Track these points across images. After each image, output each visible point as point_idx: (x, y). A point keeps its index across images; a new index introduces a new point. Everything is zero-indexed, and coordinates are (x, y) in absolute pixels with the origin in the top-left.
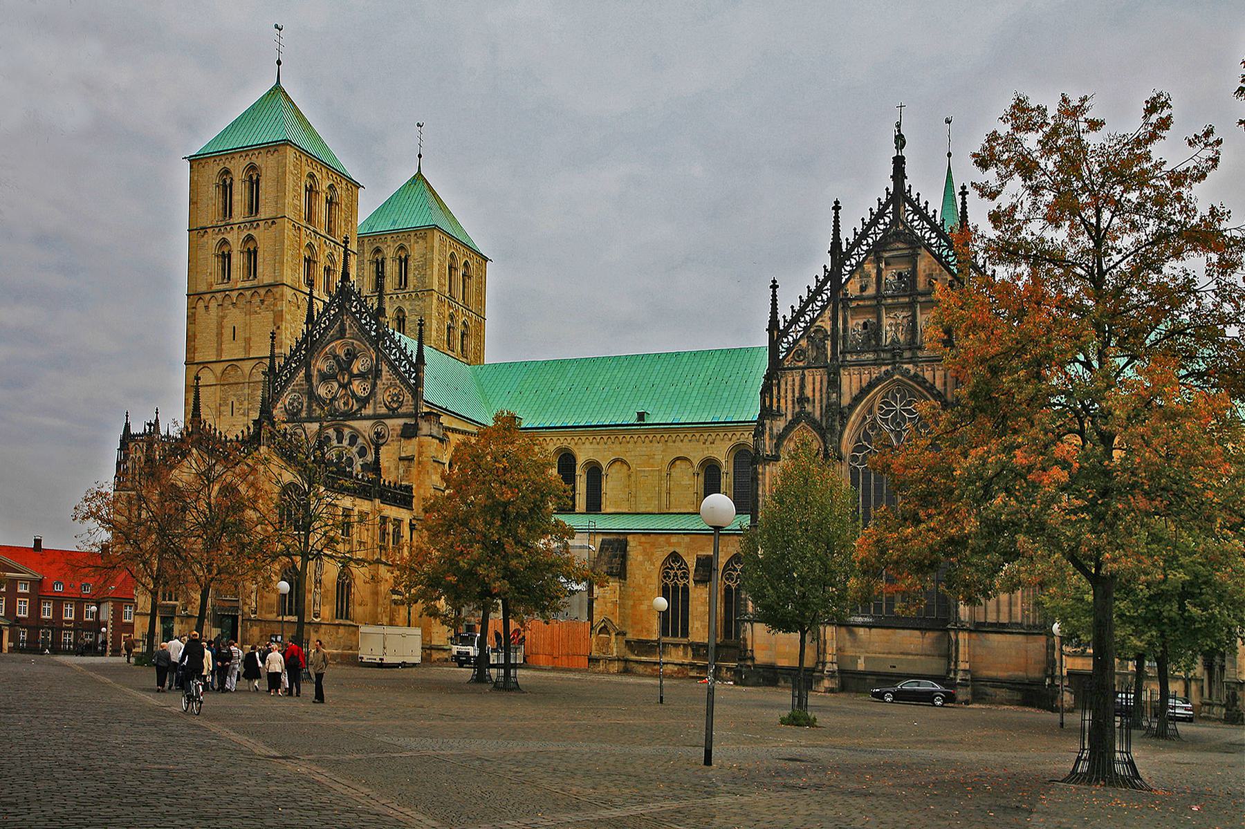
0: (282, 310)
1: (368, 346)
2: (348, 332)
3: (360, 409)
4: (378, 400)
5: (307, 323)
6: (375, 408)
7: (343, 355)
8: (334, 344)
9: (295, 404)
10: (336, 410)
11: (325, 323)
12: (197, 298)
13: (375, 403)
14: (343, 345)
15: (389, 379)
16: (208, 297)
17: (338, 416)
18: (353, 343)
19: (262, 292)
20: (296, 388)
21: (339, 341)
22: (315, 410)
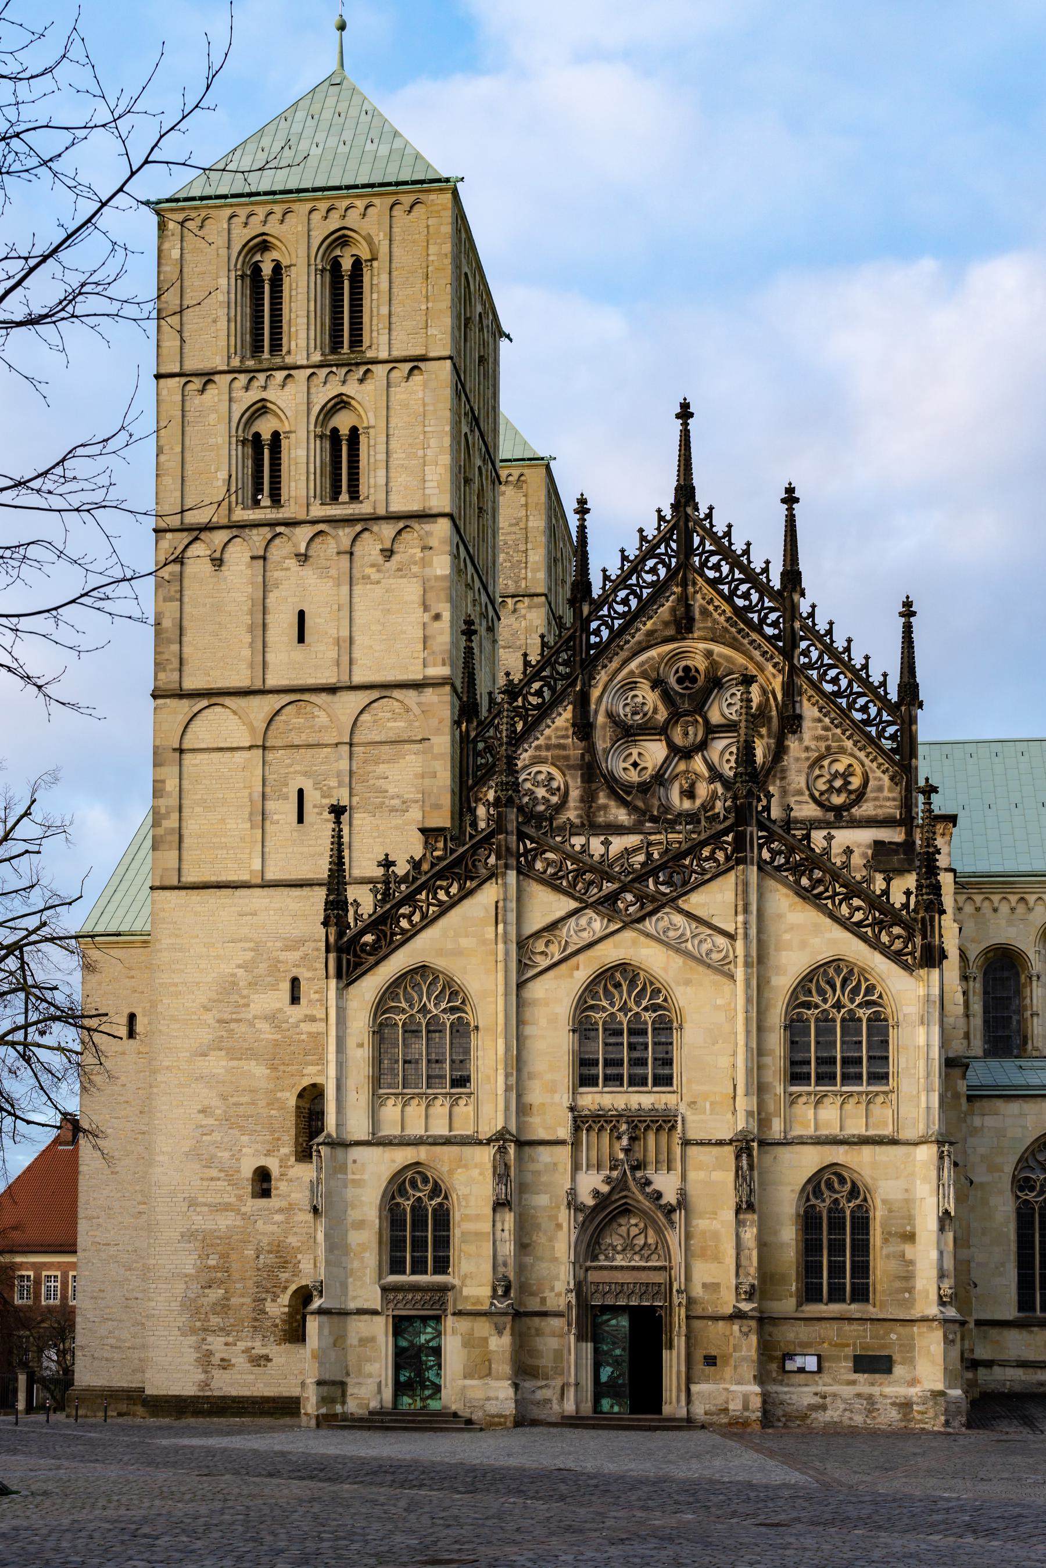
1: (760, 659)
2: (698, 624)
4: (793, 787)
5: (573, 602)
7: (672, 680)
8: (653, 653)
9: (541, 792)
10: (666, 808)
12: (185, 538)
13: (784, 792)
14: (675, 657)
15: (818, 738)
16: (221, 536)
18: (709, 654)
19: (388, 530)
20: (544, 753)
22: (605, 807)
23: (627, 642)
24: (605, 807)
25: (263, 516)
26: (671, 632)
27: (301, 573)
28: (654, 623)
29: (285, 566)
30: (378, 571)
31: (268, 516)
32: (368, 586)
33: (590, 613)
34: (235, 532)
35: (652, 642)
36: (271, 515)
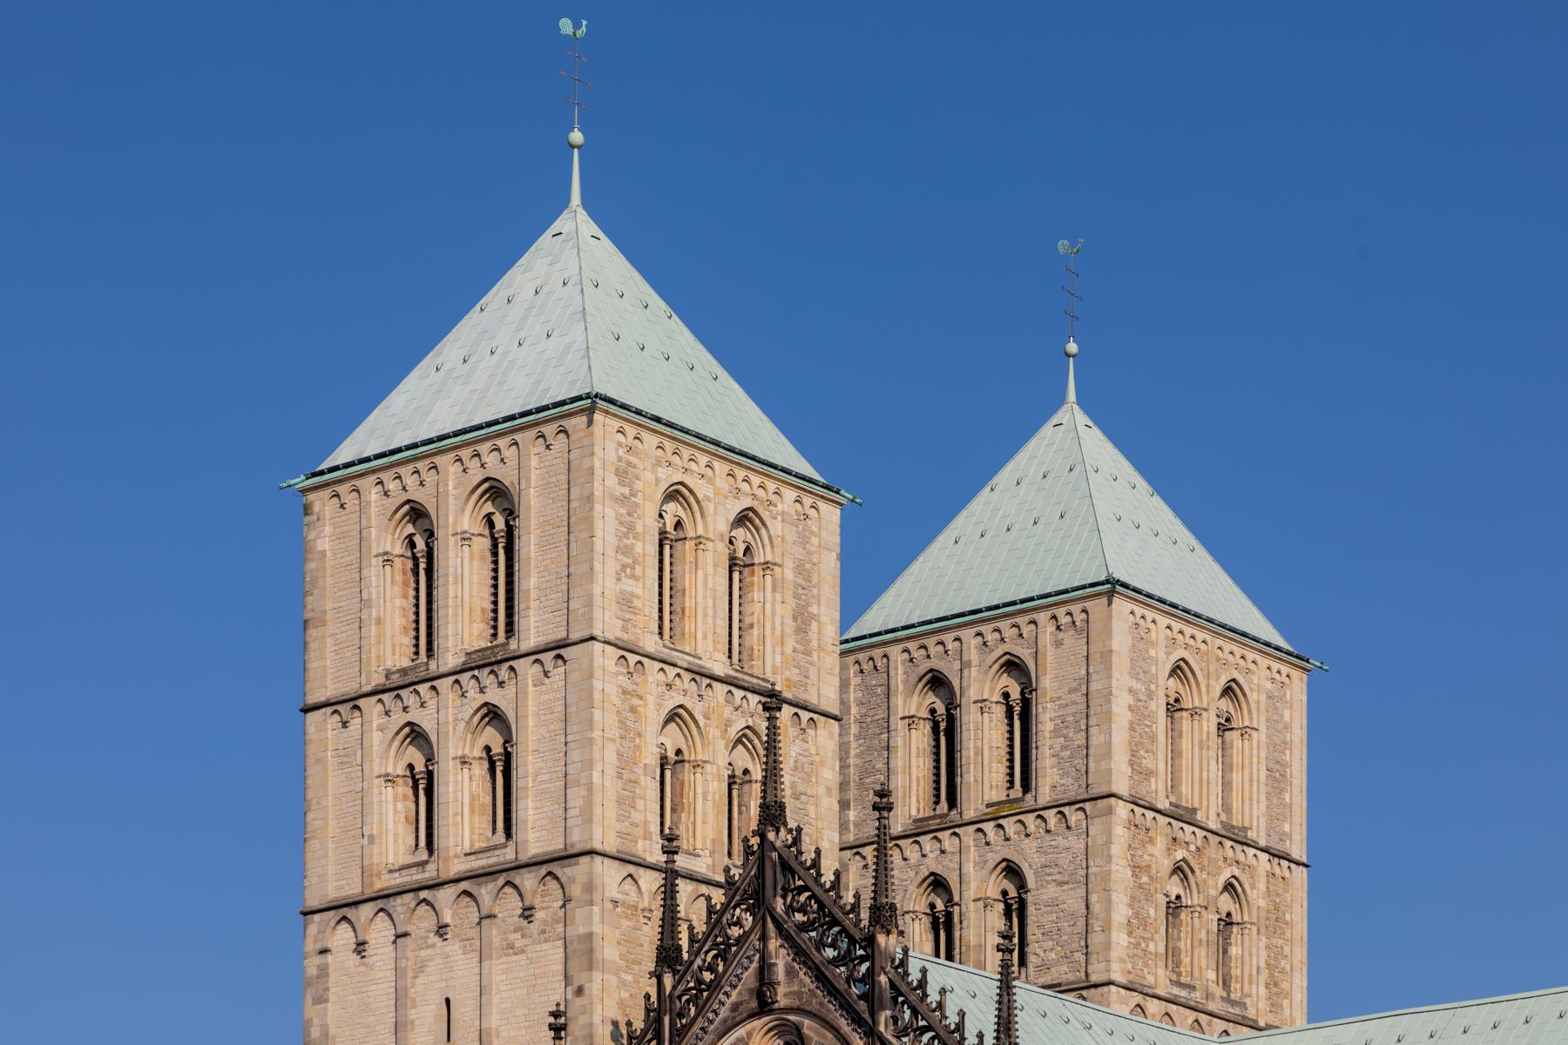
0: (590, 936)
2: (781, 990)
11: (711, 969)
16: (367, 910)
19: (528, 880)
21: (757, 1023)
23: (711, 1022)
25: (408, 879)
26: (754, 1004)
27: (447, 949)
28: (740, 993)
29: (430, 941)
30: (523, 936)
31: (415, 878)
32: (515, 958)
33: (674, 988)
34: (380, 904)
35: (738, 1019)
36: (416, 877)
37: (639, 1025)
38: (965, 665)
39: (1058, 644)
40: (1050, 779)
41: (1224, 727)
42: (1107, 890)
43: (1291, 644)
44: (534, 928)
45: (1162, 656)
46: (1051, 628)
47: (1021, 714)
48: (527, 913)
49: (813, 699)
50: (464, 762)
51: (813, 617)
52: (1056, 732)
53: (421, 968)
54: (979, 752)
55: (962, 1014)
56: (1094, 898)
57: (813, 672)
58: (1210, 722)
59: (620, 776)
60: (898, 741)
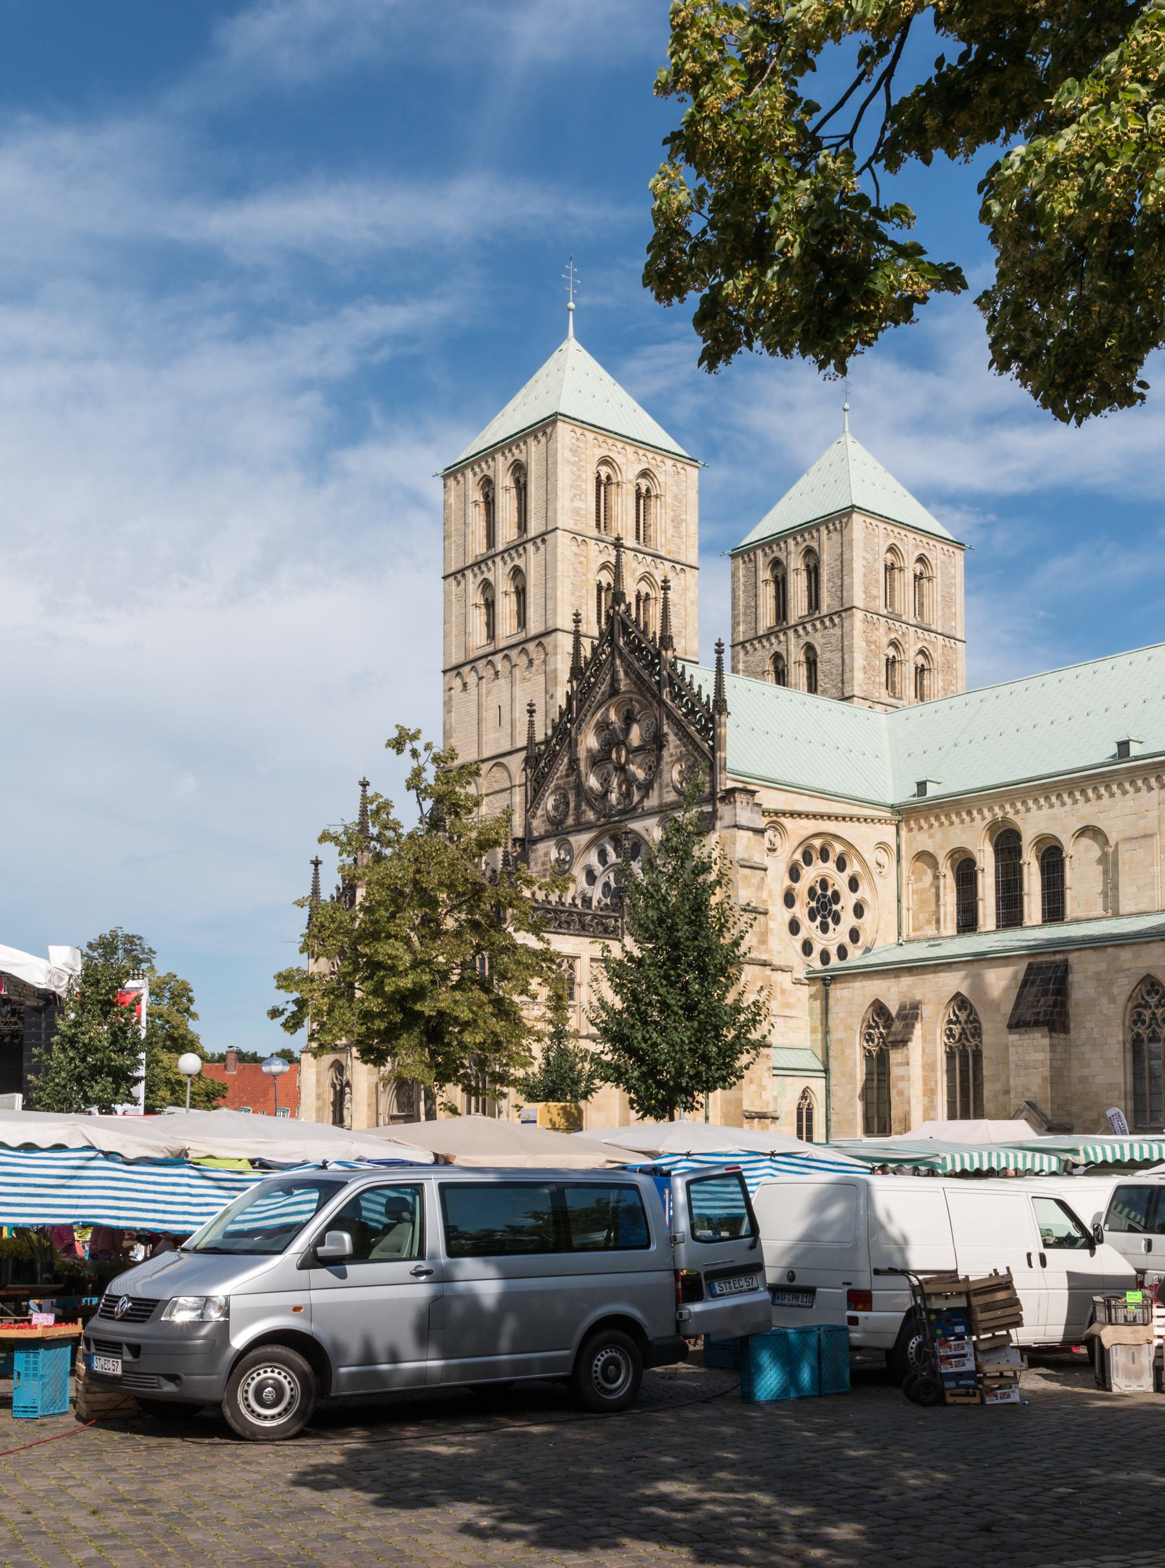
1: (650, 699)
2: (622, 683)
3: (641, 801)
6: (660, 796)
12: (454, 673)
17: (613, 816)
24: (584, 812)
37: (564, 707)
38: (788, 553)
39: (829, 539)
40: (827, 602)
41: (918, 578)
42: (852, 652)
43: (951, 533)
44: (533, 669)
45: (881, 542)
46: (826, 532)
47: (813, 572)
48: (531, 662)
49: (683, 560)
50: (506, 594)
51: (683, 520)
52: (829, 580)
53: (488, 693)
54: (796, 593)
55: (700, 687)
56: (846, 656)
57: (683, 547)
58: (909, 576)
59: (573, 594)
60: (760, 592)
